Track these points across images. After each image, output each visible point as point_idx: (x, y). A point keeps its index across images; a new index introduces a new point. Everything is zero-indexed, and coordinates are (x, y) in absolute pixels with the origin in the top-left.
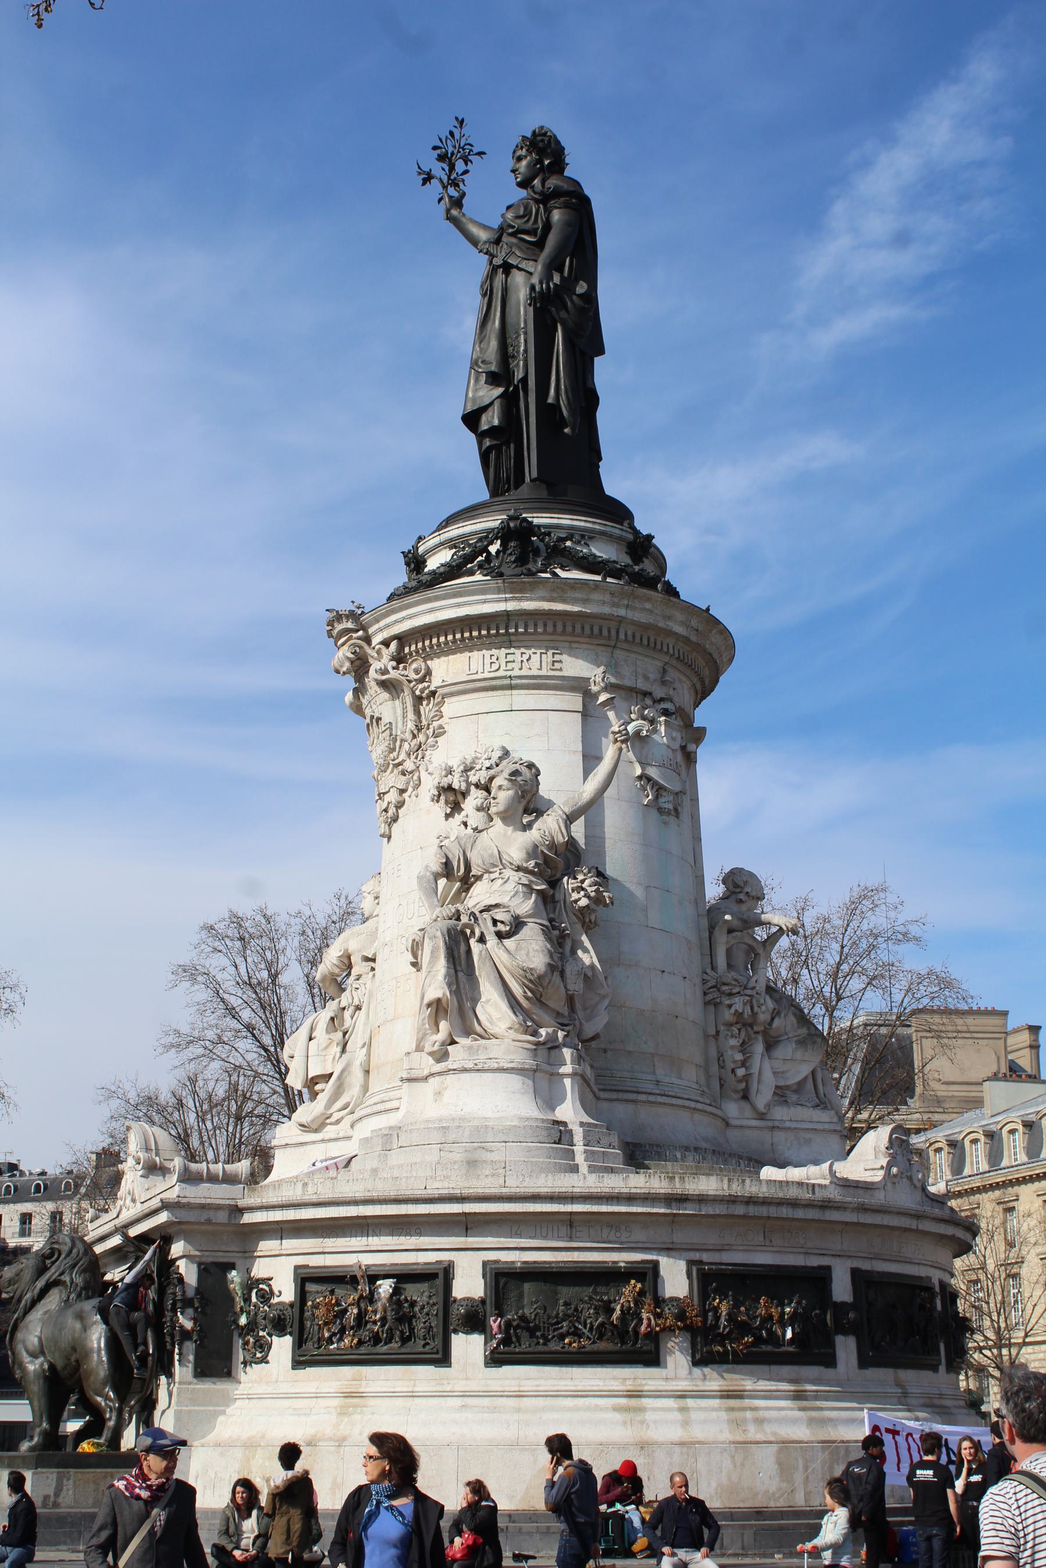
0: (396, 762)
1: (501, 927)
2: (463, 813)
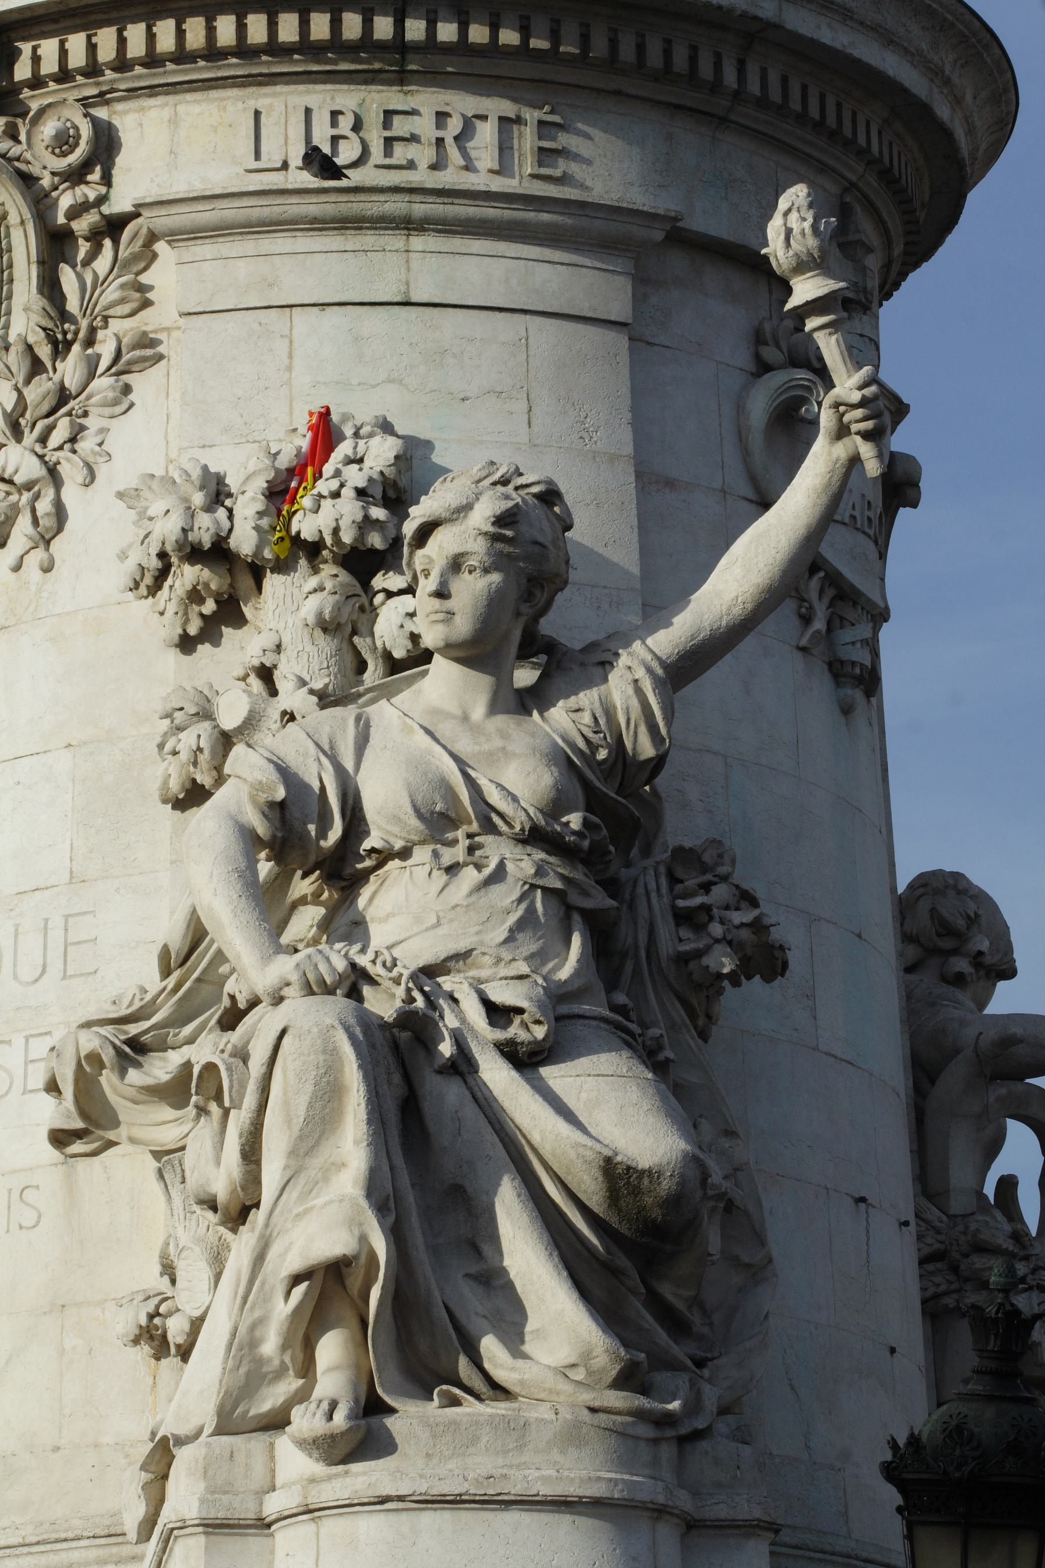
1: (514, 1031)
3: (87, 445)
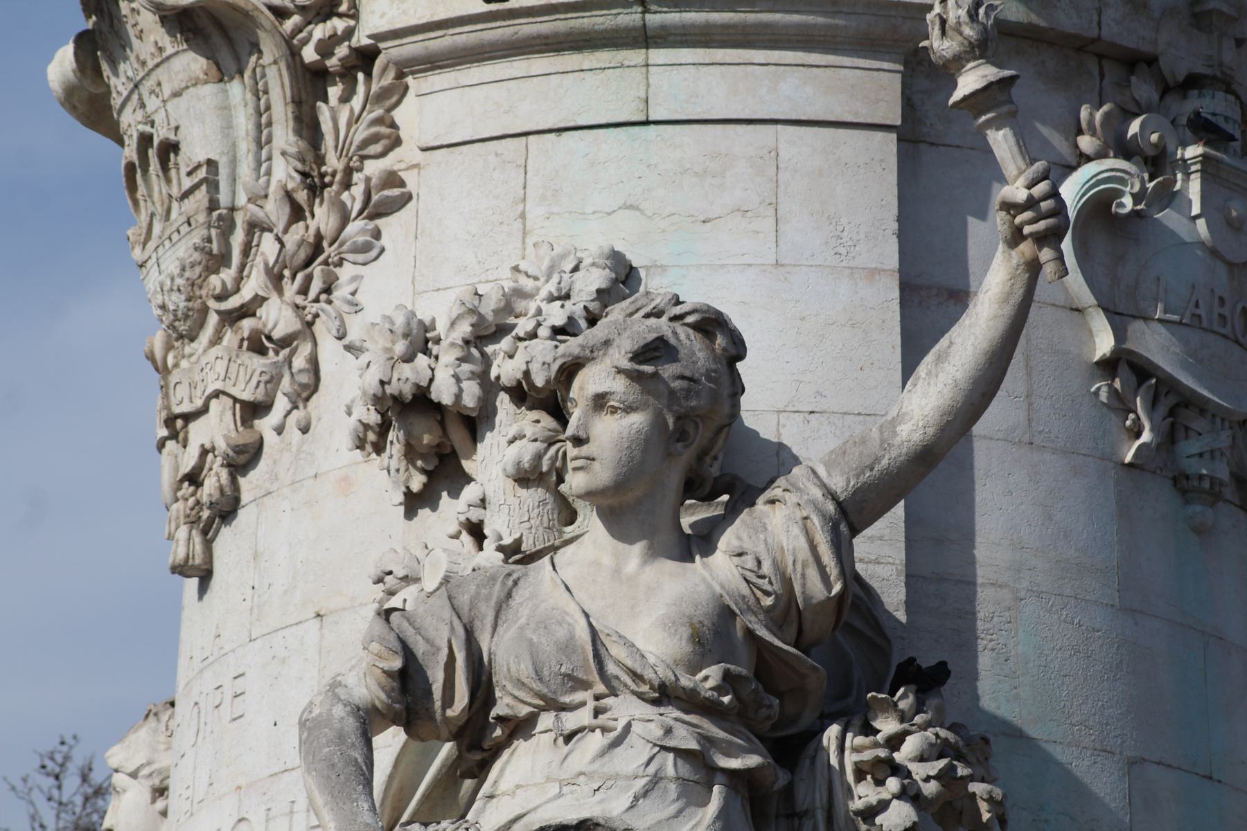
0: (233, 302)
2: (470, 493)
3: (340, 293)
